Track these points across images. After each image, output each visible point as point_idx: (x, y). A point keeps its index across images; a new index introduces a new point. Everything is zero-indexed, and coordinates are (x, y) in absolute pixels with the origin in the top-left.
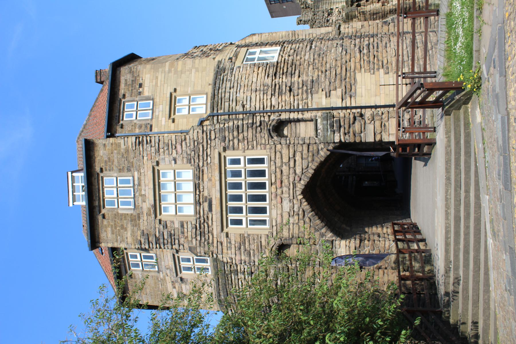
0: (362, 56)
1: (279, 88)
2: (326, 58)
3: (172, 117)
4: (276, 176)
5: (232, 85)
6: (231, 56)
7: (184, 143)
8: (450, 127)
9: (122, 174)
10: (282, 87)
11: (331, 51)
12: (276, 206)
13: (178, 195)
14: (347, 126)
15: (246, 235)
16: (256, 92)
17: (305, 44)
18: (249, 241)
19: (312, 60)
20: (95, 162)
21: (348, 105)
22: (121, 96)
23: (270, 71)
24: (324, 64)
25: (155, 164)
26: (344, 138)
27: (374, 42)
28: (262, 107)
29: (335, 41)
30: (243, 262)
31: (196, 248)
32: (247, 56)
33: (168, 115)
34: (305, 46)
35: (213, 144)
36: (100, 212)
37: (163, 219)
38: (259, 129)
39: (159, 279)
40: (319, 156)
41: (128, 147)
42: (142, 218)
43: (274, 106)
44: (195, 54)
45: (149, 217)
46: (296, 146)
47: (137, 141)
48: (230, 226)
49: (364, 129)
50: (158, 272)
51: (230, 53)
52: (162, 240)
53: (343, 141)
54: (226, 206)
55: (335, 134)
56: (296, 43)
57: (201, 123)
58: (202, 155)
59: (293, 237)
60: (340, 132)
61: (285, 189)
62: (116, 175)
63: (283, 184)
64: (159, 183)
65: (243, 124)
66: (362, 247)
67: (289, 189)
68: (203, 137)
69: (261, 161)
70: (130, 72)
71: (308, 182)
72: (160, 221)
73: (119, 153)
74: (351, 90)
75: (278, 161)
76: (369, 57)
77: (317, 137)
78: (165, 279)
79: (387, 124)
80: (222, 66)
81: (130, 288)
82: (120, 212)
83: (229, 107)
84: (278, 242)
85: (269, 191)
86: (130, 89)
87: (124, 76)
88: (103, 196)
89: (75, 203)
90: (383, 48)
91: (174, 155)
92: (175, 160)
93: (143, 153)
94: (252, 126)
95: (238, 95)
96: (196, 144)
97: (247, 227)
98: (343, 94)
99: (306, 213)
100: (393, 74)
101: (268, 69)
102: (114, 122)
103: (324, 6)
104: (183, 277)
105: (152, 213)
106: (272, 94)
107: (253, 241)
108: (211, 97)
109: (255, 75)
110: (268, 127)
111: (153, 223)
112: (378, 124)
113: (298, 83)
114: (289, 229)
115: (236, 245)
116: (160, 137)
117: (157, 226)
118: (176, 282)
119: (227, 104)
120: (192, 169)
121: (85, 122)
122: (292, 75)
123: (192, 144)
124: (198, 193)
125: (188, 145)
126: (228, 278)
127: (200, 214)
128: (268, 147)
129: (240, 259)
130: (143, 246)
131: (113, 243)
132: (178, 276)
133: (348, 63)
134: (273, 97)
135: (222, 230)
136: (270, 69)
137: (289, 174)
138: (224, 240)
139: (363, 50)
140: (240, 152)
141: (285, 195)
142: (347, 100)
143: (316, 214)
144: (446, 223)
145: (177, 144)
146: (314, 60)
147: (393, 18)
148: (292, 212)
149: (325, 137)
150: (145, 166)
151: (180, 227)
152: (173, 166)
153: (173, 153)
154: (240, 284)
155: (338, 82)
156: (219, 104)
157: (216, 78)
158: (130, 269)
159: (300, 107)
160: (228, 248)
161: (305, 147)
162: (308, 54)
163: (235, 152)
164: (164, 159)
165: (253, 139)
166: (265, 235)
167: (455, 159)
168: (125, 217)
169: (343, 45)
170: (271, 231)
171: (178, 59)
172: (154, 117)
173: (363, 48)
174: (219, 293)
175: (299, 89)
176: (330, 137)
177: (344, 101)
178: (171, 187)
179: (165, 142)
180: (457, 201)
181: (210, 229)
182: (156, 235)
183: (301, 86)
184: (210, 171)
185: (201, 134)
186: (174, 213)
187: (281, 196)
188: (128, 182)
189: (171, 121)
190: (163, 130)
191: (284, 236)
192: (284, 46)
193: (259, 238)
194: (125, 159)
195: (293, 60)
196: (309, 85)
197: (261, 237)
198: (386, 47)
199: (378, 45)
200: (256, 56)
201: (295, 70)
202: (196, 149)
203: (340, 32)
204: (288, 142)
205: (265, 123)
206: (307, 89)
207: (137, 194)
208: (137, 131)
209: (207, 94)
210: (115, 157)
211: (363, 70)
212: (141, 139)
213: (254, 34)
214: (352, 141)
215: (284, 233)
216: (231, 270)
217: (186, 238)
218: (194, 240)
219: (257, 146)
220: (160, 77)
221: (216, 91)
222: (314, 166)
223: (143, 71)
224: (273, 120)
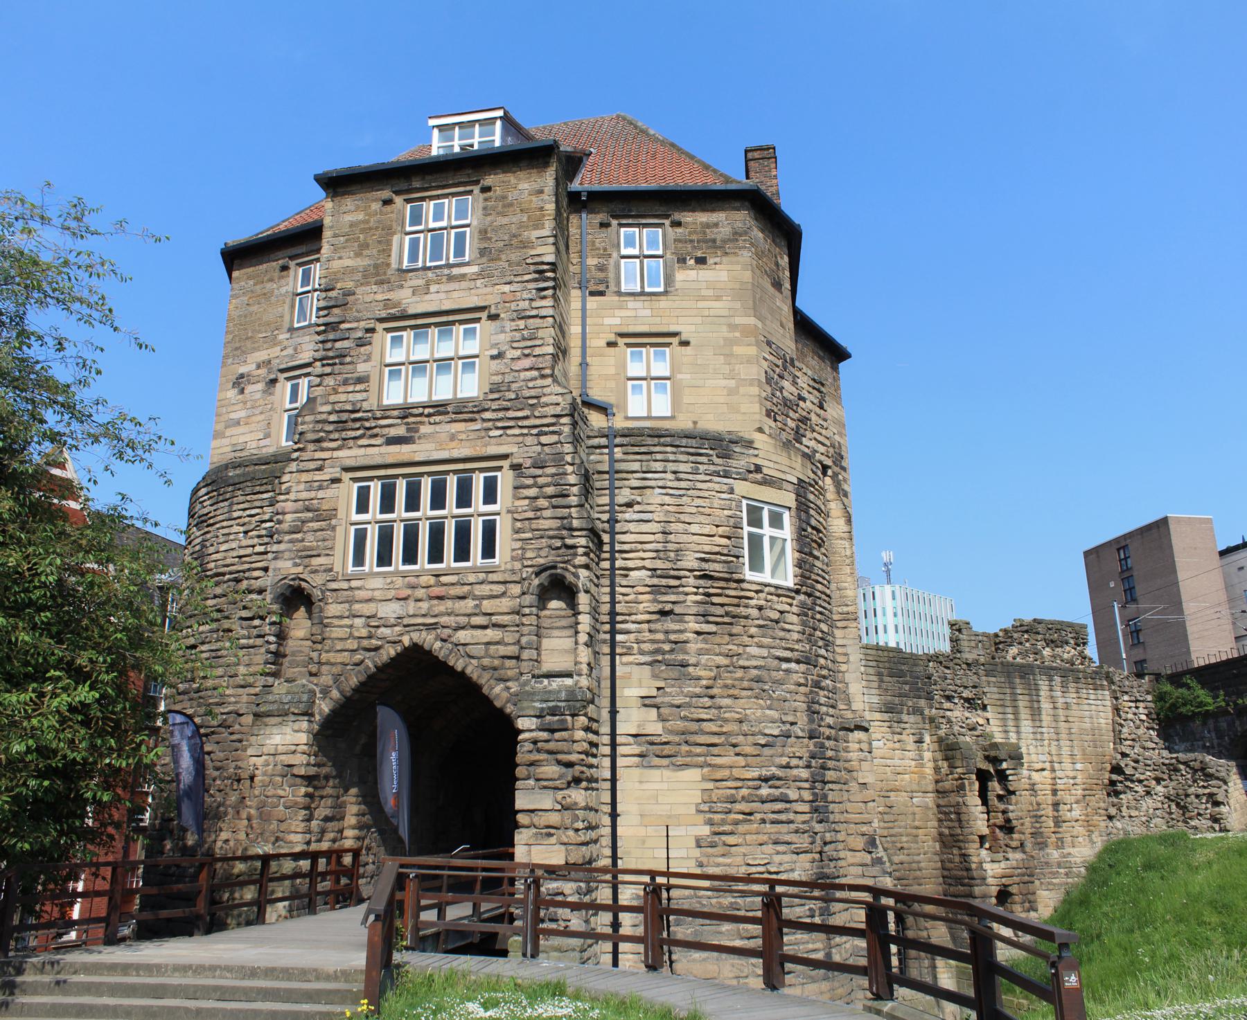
0: (750, 783)
2: (749, 697)
3: (621, 341)
4: (453, 584)
6: (765, 471)
7: (535, 373)
8: (356, 981)
9: (476, 235)
10: (673, 593)
11: (770, 708)
12: (391, 586)
13: (426, 367)
14: (551, 746)
15: (334, 522)
18: (322, 530)
19: (741, 663)
20: (504, 172)
21: (620, 750)
22: (677, 216)
23: (716, 564)
24: (731, 692)
25: (493, 311)
26: (525, 740)
27: (796, 813)
28: (626, 547)
30: (280, 517)
32: (766, 508)
33: (625, 330)
35: (529, 440)
36: (397, 193)
37: (376, 337)
38: (558, 543)
39: (277, 332)
41: (533, 248)
42: (381, 290)
43: (626, 576)
45: (382, 304)
46: (517, 629)
47: (546, 267)
48: (356, 485)
49: (545, 787)
50: (292, 330)
51: (777, 466)
52: (331, 336)
53: (520, 737)
54: (473, 470)
55: (534, 719)
59: (326, 626)
60: (540, 730)
61: (424, 606)
62: (475, 223)
63: (435, 602)
64: (453, 323)
65: (570, 507)
66: (292, 780)
67: (424, 616)
68: (546, 417)
69: (489, 551)
70: (735, 233)
71: (437, 657)
73: (521, 225)
75: (485, 589)
79: (553, 840)
81: (261, 267)
82: (396, 239)
83: (628, 472)
84: (317, 593)
85: (424, 570)
86: (694, 237)
87: (727, 219)
88: (431, 198)
89: (436, 131)
90: (772, 837)
92: (499, 356)
94: (565, 528)
95: (658, 491)
97: (352, 524)
98: (648, 738)
99: (373, 653)
100: (696, 858)
101: (723, 558)
102: (617, 207)
103: (995, 690)
104: (277, 385)
106: (655, 570)
107: (321, 538)
108: (658, 429)
109: (706, 530)
110: (562, 565)
111: (369, 315)
112: (554, 818)
114: (341, 617)
115: (315, 502)
119: (636, 466)
120: (478, 397)
121: (652, 132)
122: (704, 616)
123: (533, 393)
124: (427, 411)
125: (531, 384)
127: (382, 418)
128: (518, 565)
129: (286, 510)
131: (331, 227)
132: (279, 374)
133: (732, 751)
134: (649, 573)
136: (721, 565)
138: (326, 475)
139: (770, 787)
141: (411, 607)
142: (635, 746)
143: (371, 677)
144: (167, 966)
145: (534, 359)
146: (744, 668)
147: (883, 863)
148: (376, 624)
149: (531, 695)
150: (489, 290)
154: (253, 512)
156: (637, 449)
158: (300, 265)
159: (619, 637)
161: (512, 650)
162: (764, 652)
164: (502, 332)
165: (537, 530)
167: (278, 989)
168: (384, 250)
171: (769, 343)
172: (622, 299)
175: (667, 632)
176: (528, 708)
177: (631, 740)
178: (445, 349)
179: (540, 331)
180: (195, 992)
181: (351, 443)
182: (343, 322)
183: (673, 637)
184: (472, 435)
185: (552, 413)
186: (388, 360)
187: (412, 599)
188: (460, 251)
189: (612, 338)
190: (589, 321)
191: (328, 607)
192: (793, 594)
193: (327, 552)
194: (506, 243)
195: (746, 617)
197: (328, 555)
198: (775, 843)
199: (782, 822)
200: (767, 531)
201: (717, 623)
202: (521, 403)
203: (852, 731)
204: (527, 611)
206: (664, 653)
207: (430, 274)
209: (672, 418)
210: (514, 219)
211: (710, 785)
213: (849, 521)
215: (334, 606)
218: (328, 408)
220: (720, 307)
221: (668, 439)
222: (472, 671)
223: (738, 263)
224: (577, 576)
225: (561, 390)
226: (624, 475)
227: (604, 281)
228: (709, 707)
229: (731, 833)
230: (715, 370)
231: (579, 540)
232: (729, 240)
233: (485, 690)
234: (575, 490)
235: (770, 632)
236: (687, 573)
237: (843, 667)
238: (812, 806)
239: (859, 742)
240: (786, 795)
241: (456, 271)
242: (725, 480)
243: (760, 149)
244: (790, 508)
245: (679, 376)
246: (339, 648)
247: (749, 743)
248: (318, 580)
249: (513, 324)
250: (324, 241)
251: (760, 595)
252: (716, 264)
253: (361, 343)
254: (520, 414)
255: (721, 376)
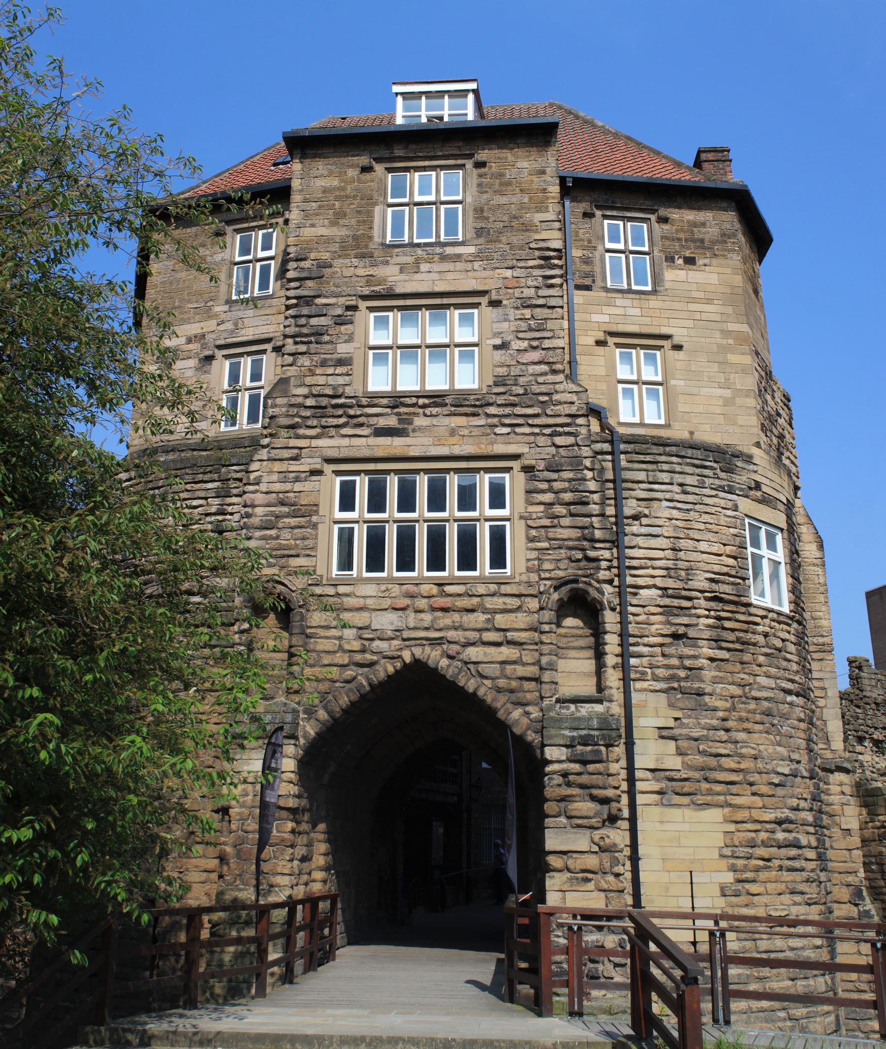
0: (768, 826)
1: (682, 608)
2: (760, 732)
3: (611, 341)
4: (459, 595)
5: (689, 489)
6: (764, 488)
7: (544, 368)
9: (471, 213)
10: (686, 615)
11: (779, 744)
13: (417, 352)
14: (584, 779)
15: (314, 519)
16: (672, 549)
17: (797, 678)
18: (301, 527)
19: (754, 693)
21: (640, 786)
22: (663, 212)
23: (725, 586)
24: (747, 725)
25: (494, 297)
26: (554, 773)
27: (806, 859)
28: (635, 563)
29: (806, 757)
30: (249, 510)
31: (285, 394)
32: (764, 528)
33: (614, 328)
34: (791, 677)
35: (541, 441)
37: (359, 316)
38: (579, 555)
39: (210, 304)
40: (509, 706)
41: (536, 232)
42: (362, 264)
43: (636, 594)
44: (769, 397)
46: (535, 647)
47: (552, 254)
48: (338, 480)
49: (579, 826)
50: (229, 302)
52: (305, 311)
53: (548, 769)
55: (564, 749)
56: (799, 654)
57: (595, 412)
58: (515, 412)
61: (427, 618)
62: (469, 199)
63: (439, 614)
64: (447, 306)
65: (590, 516)
67: (427, 629)
68: (559, 416)
69: (498, 560)
70: (723, 235)
71: (444, 676)
72: (354, 308)
73: (521, 206)
74: (677, 794)
76: (765, 844)
77: (558, 701)
78: (210, 317)
79: (591, 886)
80: (739, 464)
81: (189, 230)
83: (633, 482)
86: (682, 235)
90: (789, 885)
91: (516, 345)
92: (504, 346)
93: (521, 268)
94: (585, 539)
95: (665, 504)
96: (542, 398)
97: (336, 522)
98: (667, 773)
101: (732, 579)
104: (214, 362)
105: (372, 288)
106: (666, 589)
107: (300, 535)
108: (660, 437)
109: (715, 548)
110: (584, 579)
111: (349, 291)
112: (592, 862)
113: (695, 657)
114: (328, 627)
115: (291, 495)
116: (559, 310)
117: (342, 301)
118: (202, 345)
119: (642, 476)
120: (480, 389)
122: (716, 641)
123: (544, 389)
124: (421, 401)
125: (541, 379)
126: (210, 472)
127: (368, 406)
128: (534, 577)
129: (257, 503)
130: (292, 265)
132: (216, 351)
133: (748, 790)
134: (660, 592)
135: (329, 461)
136: (731, 587)
137: (466, 630)
138: (305, 465)
139: (784, 831)
140: (521, 506)
141: (412, 619)
142: (652, 782)
143: (363, 697)
145: (543, 352)
146: (756, 699)
147: (872, 917)
148: (370, 636)
149: (558, 722)
150: (488, 273)
151: (339, 356)
152: (489, 342)
153: (520, 343)
154: (195, 503)
155: (700, 760)
156: (642, 458)
157: (707, 448)
158: (238, 231)
159: (633, 661)
160: (282, 475)
162: (771, 683)
163: (521, 496)
164: (505, 320)
165: (554, 539)
166: (315, 566)
168: (364, 221)
169: (796, 776)
170: (324, 582)
171: (757, 353)
172: (610, 295)
173: (790, 831)
174: (172, 450)
175: (681, 657)
176: (556, 736)
177: (649, 775)
178: (437, 335)
179: (549, 322)
181: (333, 431)
182: (319, 296)
183: (687, 663)
184: (476, 432)
185: (567, 412)
186: (372, 342)
187: (411, 609)
188: (451, 229)
189: (601, 336)
190: (577, 316)
192: (790, 622)
193: (308, 552)
194: (506, 224)
195: (754, 644)
196: (689, 684)
197: (309, 556)
198: (793, 892)
199: (796, 870)
200: (764, 551)
201: (729, 650)
202: (531, 399)
204: (546, 628)
205: (592, 571)
206: (679, 679)
207: (419, 251)
208: (576, 253)
209: (667, 426)
211: (732, 827)
212: (556, 262)
213: (821, 547)
214: (549, 792)
216: (229, 480)
217: (310, 370)
218: (304, 391)
219: (535, 549)
220: (712, 310)
221: (674, 449)
222: (485, 691)
223: (728, 266)
224: (603, 593)
225: (576, 388)
226: (630, 485)
227: (590, 275)
228: (725, 742)
229: (754, 881)
230: (709, 377)
231: (602, 552)
232: (717, 241)
233: (501, 714)
234: (596, 497)
235: (775, 661)
236: (699, 594)
237: (821, 702)
238: (817, 853)
239: (841, 785)
240: (798, 840)
241: (449, 250)
242: (730, 496)
243: (714, 150)
244: (782, 530)
245: (673, 382)
246: (326, 662)
247: (764, 781)
248: (298, 583)
249: (517, 312)
250: (292, 205)
251: (765, 620)
252: (705, 265)
253: (340, 321)
254: (530, 411)
255: (716, 385)
